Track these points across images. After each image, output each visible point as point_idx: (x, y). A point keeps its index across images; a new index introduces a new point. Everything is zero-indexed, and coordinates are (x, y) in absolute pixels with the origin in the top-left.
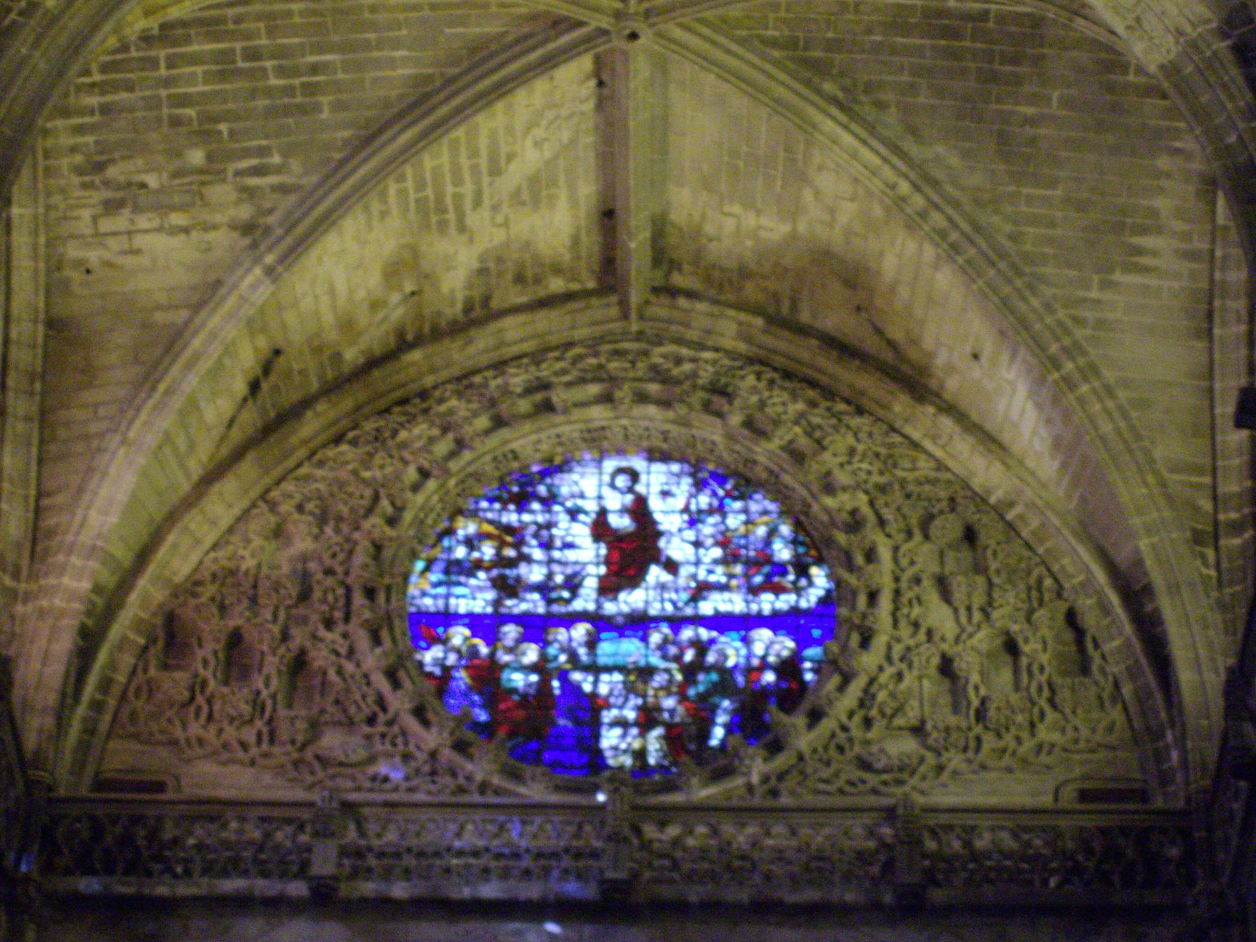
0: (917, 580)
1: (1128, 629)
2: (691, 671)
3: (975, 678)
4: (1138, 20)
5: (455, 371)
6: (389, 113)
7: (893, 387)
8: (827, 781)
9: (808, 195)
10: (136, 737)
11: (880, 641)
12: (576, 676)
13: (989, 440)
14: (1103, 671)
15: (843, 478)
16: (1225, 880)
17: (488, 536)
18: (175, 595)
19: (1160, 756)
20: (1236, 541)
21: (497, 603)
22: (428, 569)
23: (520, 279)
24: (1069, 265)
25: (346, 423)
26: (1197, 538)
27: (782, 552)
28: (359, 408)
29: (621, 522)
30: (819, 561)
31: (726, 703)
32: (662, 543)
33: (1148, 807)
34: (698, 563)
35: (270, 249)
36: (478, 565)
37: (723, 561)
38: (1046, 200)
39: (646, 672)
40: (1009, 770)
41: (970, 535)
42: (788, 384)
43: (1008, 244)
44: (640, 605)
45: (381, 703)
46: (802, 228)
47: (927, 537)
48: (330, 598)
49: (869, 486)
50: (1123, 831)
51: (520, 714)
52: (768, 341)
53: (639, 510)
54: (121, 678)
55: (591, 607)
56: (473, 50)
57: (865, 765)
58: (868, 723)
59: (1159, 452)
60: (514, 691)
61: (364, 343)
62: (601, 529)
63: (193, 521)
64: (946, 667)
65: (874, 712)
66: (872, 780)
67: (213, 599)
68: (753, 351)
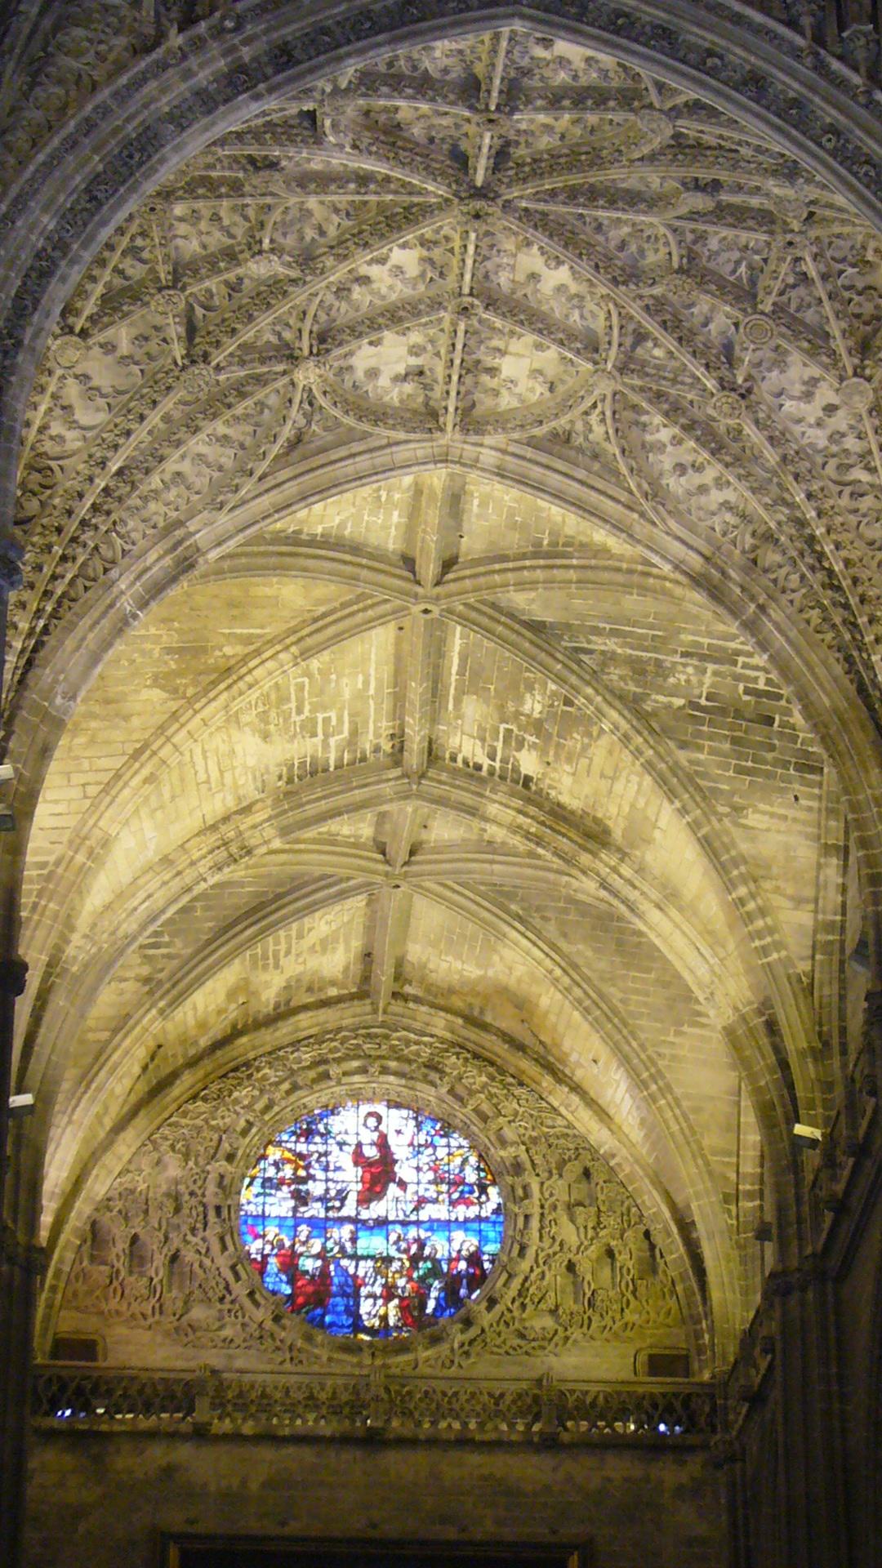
0: (555, 1208)
1: (682, 1250)
2: (415, 1260)
3: (588, 1277)
4: (712, 994)
5: (268, 1048)
6: (238, 913)
7: (544, 1072)
8: (498, 1347)
9: (496, 958)
10: (77, 1309)
11: (531, 1253)
12: (344, 1262)
13: (603, 1114)
14: (665, 1272)
15: (509, 1134)
16: (734, 1433)
17: (289, 1161)
18: (97, 1210)
19: (698, 1335)
20: (750, 1204)
21: (295, 1209)
22: (250, 1184)
23: (310, 989)
24: (656, 1021)
25: (200, 1085)
26: (726, 1199)
27: (471, 1176)
28: (207, 1075)
29: (371, 1152)
30: (494, 1183)
31: (436, 1284)
32: (396, 1168)
33: (692, 1380)
34: (418, 1183)
35: (161, 998)
36: (282, 1182)
37: (435, 1182)
38: (643, 980)
39: (388, 1260)
40: (607, 1340)
41: (587, 1173)
42: (476, 1062)
43: (619, 1005)
44: (383, 1214)
45: (227, 1288)
46: (490, 973)
47: (561, 1176)
48: (194, 1213)
49: (526, 1139)
50: (676, 1395)
51: (310, 1289)
52: (465, 1033)
53: (383, 1144)
54: (67, 1269)
55: (353, 1214)
56: (293, 879)
57: (522, 1336)
58: (523, 1306)
59: (706, 1142)
60: (307, 1272)
61: (211, 1034)
62: (358, 1158)
63: (108, 1159)
64: (571, 1267)
65: (527, 1301)
66: (527, 1347)
67: (120, 1212)
68: (455, 1038)
